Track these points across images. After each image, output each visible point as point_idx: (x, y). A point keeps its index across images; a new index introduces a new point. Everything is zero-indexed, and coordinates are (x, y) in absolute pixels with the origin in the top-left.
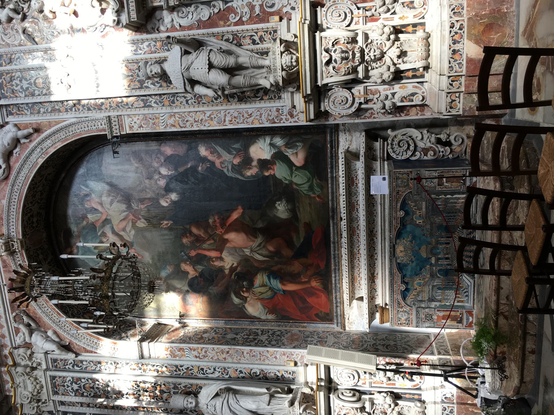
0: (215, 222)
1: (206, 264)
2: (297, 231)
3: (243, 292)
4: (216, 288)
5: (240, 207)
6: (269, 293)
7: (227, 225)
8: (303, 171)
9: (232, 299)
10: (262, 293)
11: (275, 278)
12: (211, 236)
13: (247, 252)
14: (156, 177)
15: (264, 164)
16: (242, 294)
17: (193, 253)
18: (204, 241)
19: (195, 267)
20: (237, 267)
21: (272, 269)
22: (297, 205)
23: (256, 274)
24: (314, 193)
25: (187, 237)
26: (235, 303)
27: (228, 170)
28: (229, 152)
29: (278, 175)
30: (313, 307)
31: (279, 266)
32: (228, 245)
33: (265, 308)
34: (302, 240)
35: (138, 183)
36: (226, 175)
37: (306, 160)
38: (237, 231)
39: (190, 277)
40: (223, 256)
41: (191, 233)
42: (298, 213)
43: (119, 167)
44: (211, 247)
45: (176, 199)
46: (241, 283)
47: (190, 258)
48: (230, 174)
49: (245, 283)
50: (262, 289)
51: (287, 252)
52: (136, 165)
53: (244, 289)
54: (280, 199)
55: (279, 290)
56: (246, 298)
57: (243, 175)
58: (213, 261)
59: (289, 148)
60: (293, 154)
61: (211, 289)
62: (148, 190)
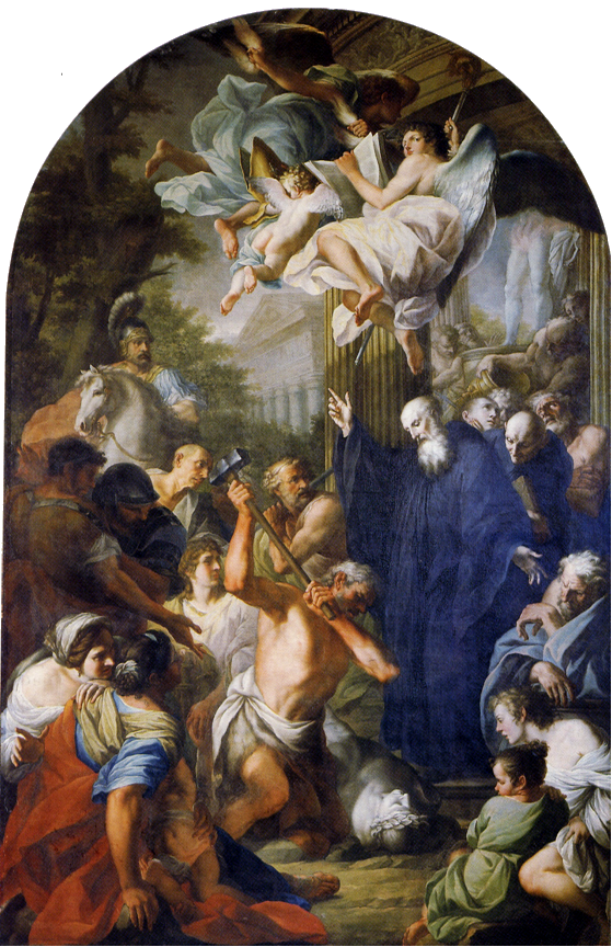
0: (344, 579)
1: (200, 535)
2: (312, 854)
3: (101, 657)
4: (114, 562)
5: (392, 671)
6: (95, 748)
7: (336, 624)
8: (505, 883)
9: (74, 611)
10: (95, 723)
11: (150, 770)
12: (298, 562)
13: (241, 683)
14: (500, 397)
15: (530, 762)
16: (93, 652)
17: (237, 494)
18: (280, 538)
19: (188, 497)
20: (188, 642)
21: (182, 763)
22: (398, 861)
23: (164, 708)
24: (433, 917)
25: (296, 479)
26: (60, 625)
27: (514, 643)
28: (570, 655)
29: (492, 806)
30: (50, 893)
31: (191, 787)
32: (266, 620)
33: (41, 726)
34: (280, 868)
35: (481, 330)
36: (499, 635)
37: (540, 899)
38: (315, 653)
39: (154, 475)
40: (228, 597)
41: (310, 495)
42: (369, 862)
43: (536, 273)
44: (259, 560)
45: (424, 458)
46: (132, 652)
47: (221, 481)
48: (501, 649)
49: (131, 665)
50: (109, 724)
51: (238, 816)
52: (540, 337)
53: (109, 662)
54: (416, 805)
55: (106, 781)
56: (79, 665)
57: (494, 692)
58: (208, 561)
59: (577, 847)
60: (559, 857)
61: (108, 546)
62: (456, 362)
